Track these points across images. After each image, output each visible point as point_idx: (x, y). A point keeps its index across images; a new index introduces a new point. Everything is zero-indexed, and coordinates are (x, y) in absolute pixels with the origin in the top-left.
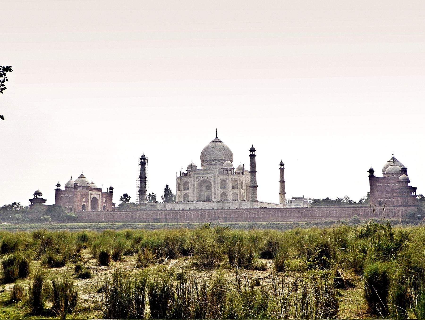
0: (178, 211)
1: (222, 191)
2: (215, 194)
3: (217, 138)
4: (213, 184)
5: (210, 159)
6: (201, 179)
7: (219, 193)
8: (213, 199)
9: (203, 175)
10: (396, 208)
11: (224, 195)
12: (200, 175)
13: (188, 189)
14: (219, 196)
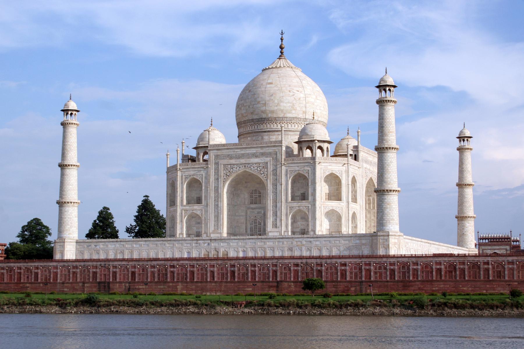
0: (169, 263)
1: (295, 204)
5: (264, 116)
8: (269, 227)
9: (243, 161)
12: (233, 161)
13: (199, 201)
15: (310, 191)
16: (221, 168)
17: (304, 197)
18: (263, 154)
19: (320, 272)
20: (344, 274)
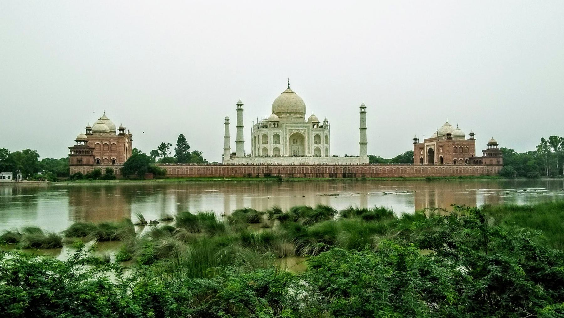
1: (316, 145)
2: (309, 148)
3: (289, 88)
4: (307, 138)
6: (294, 132)
7: (313, 148)
10: (489, 167)
11: (318, 150)
13: (276, 142)
14: (313, 151)
15: (322, 141)
16: (288, 130)
17: (316, 143)
18: (304, 126)
19: (349, 170)
20: (357, 171)
